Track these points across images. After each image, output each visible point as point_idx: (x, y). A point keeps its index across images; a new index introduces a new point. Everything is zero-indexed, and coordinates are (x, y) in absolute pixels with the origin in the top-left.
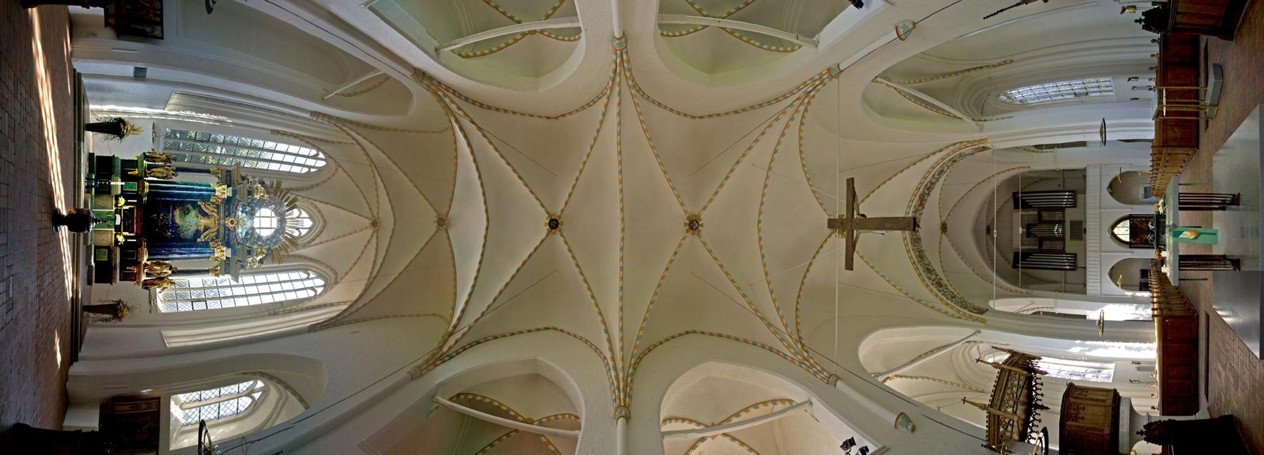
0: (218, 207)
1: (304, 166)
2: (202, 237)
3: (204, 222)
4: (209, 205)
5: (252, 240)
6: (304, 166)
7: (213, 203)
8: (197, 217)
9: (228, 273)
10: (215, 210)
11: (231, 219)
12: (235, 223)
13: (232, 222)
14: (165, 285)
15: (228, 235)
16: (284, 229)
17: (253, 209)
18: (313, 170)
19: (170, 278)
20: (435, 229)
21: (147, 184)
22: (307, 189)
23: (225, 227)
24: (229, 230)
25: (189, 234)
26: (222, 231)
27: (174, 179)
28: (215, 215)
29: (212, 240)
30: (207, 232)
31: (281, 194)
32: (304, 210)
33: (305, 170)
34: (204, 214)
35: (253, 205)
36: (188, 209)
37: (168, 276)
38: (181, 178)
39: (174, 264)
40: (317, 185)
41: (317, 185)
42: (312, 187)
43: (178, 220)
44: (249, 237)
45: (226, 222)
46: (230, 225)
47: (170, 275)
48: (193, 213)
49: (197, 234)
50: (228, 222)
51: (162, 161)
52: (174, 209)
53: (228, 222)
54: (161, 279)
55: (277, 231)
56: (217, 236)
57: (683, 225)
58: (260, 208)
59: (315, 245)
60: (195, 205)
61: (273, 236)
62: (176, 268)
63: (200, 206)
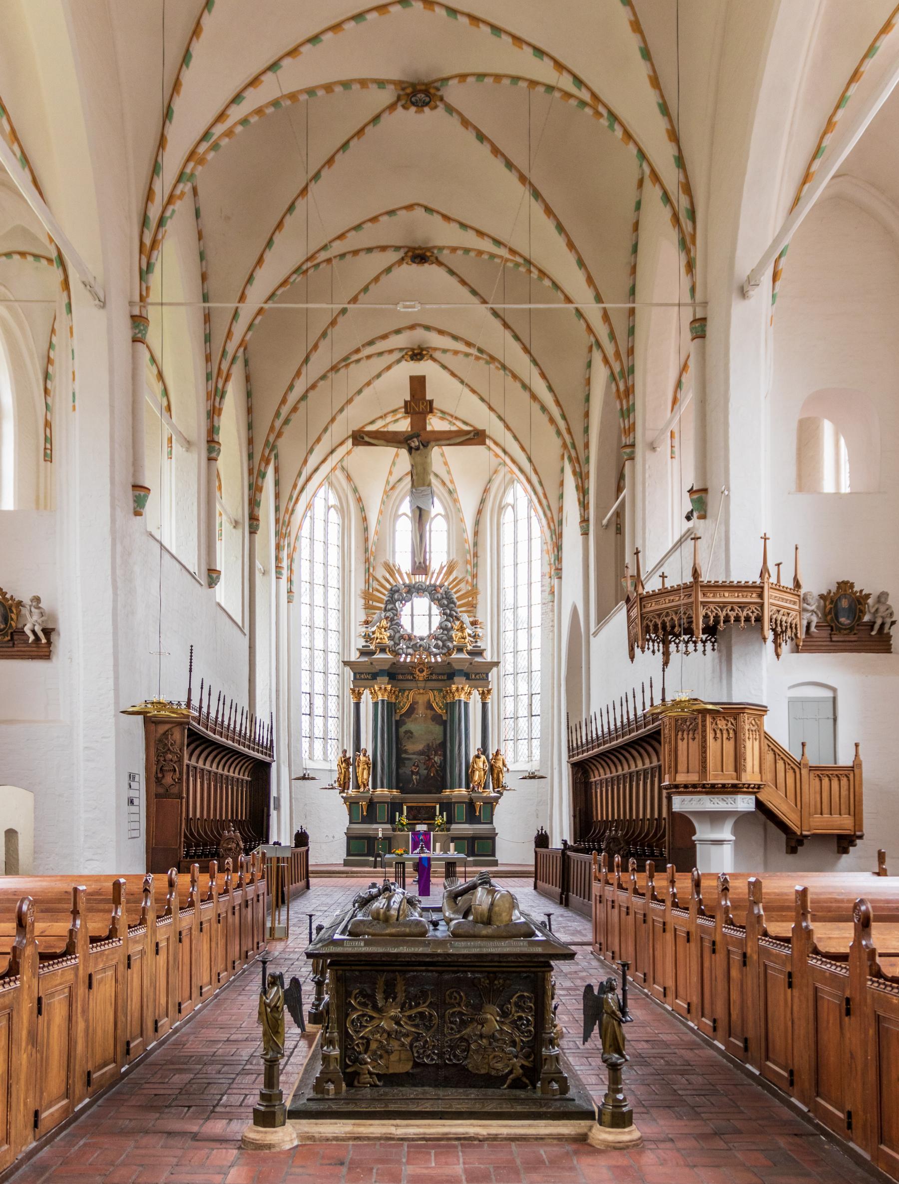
0: (402, 691)
1: (326, 521)
2: (439, 711)
3: (421, 711)
4: (400, 702)
5: (445, 637)
6: (326, 521)
7: (397, 697)
8: (416, 719)
9: (487, 676)
10: (406, 694)
11: (418, 673)
12: (421, 666)
13: (421, 671)
14: (500, 764)
15: (438, 674)
16: (430, 585)
17: (402, 637)
18: (333, 500)
19: (491, 757)
20: (430, 362)
21: (379, 791)
22: (363, 509)
23: (427, 680)
24: (431, 674)
25: (438, 729)
26: (431, 684)
27: (370, 753)
28: (412, 693)
29: (444, 697)
30: (434, 705)
31: (378, 591)
32: (397, 510)
33: (334, 516)
34: (412, 710)
35: (397, 635)
36: (406, 732)
37: (487, 757)
38: (367, 743)
39: (473, 753)
40: (355, 490)
41: (355, 490)
42: (359, 500)
43: (420, 747)
44: (440, 643)
45: (421, 679)
46: (425, 673)
47: (487, 757)
48: (410, 726)
49: (437, 719)
50: (421, 676)
51: (348, 769)
52: (406, 752)
53: (421, 676)
54: (492, 768)
55: (433, 599)
56: (441, 690)
57: (420, 116)
58: (402, 627)
59: (452, 482)
60: (399, 724)
61: (441, 606)
62: (478, 750)
63: (401, 716)
